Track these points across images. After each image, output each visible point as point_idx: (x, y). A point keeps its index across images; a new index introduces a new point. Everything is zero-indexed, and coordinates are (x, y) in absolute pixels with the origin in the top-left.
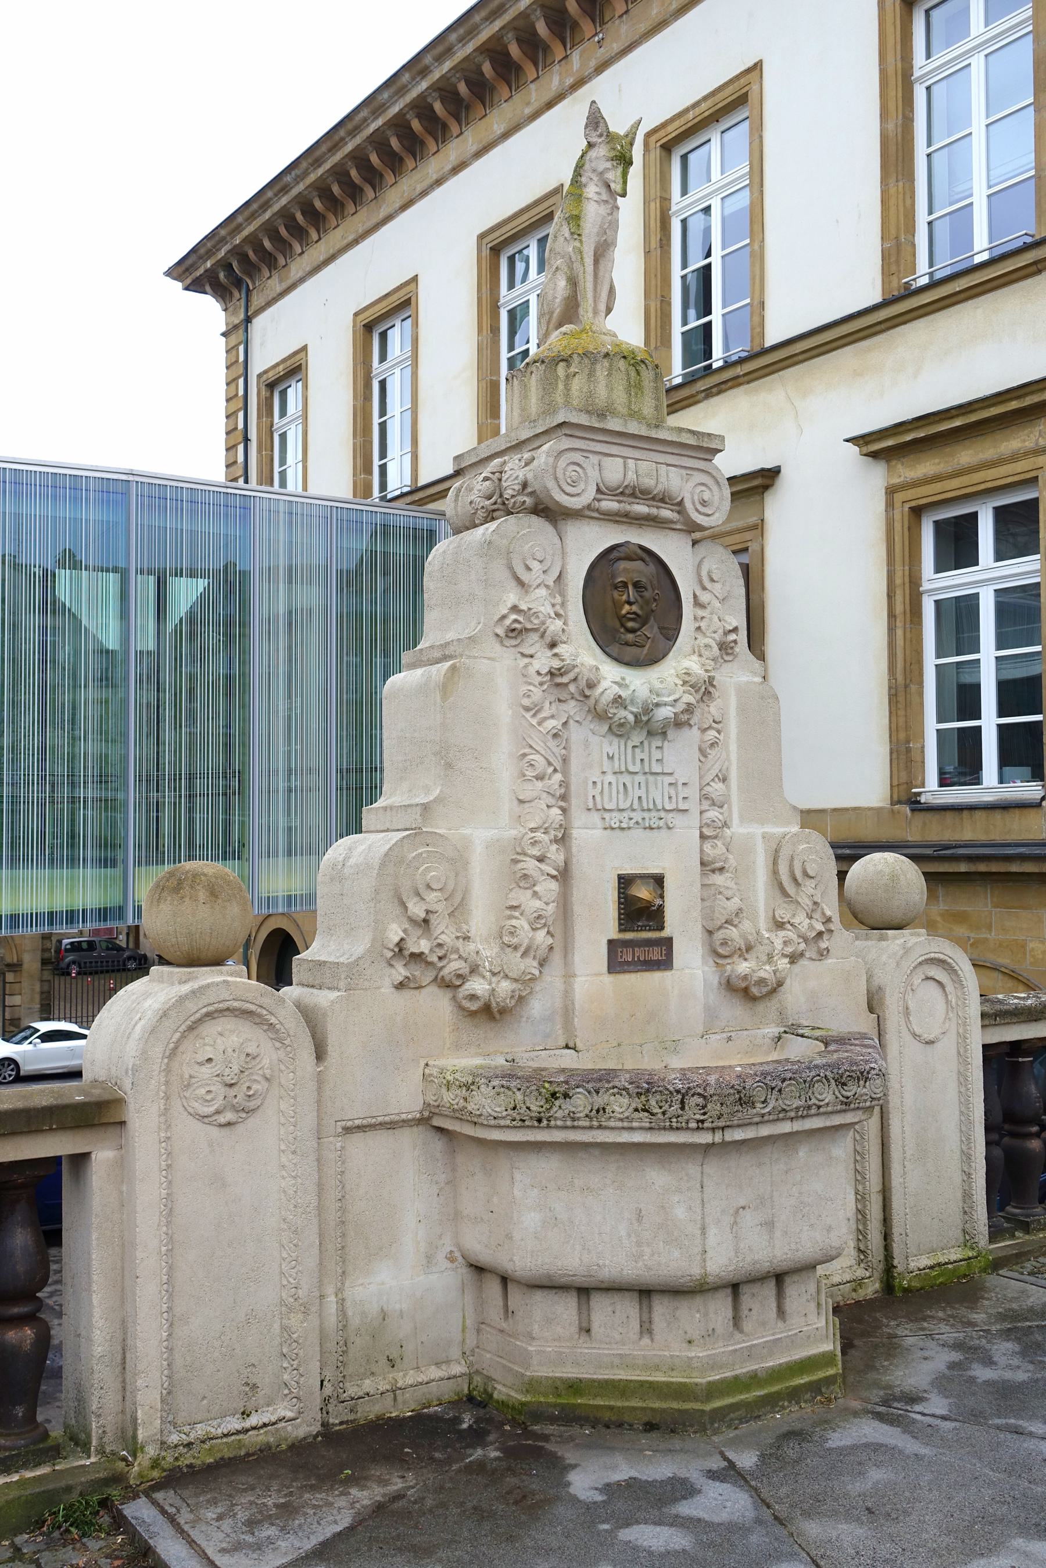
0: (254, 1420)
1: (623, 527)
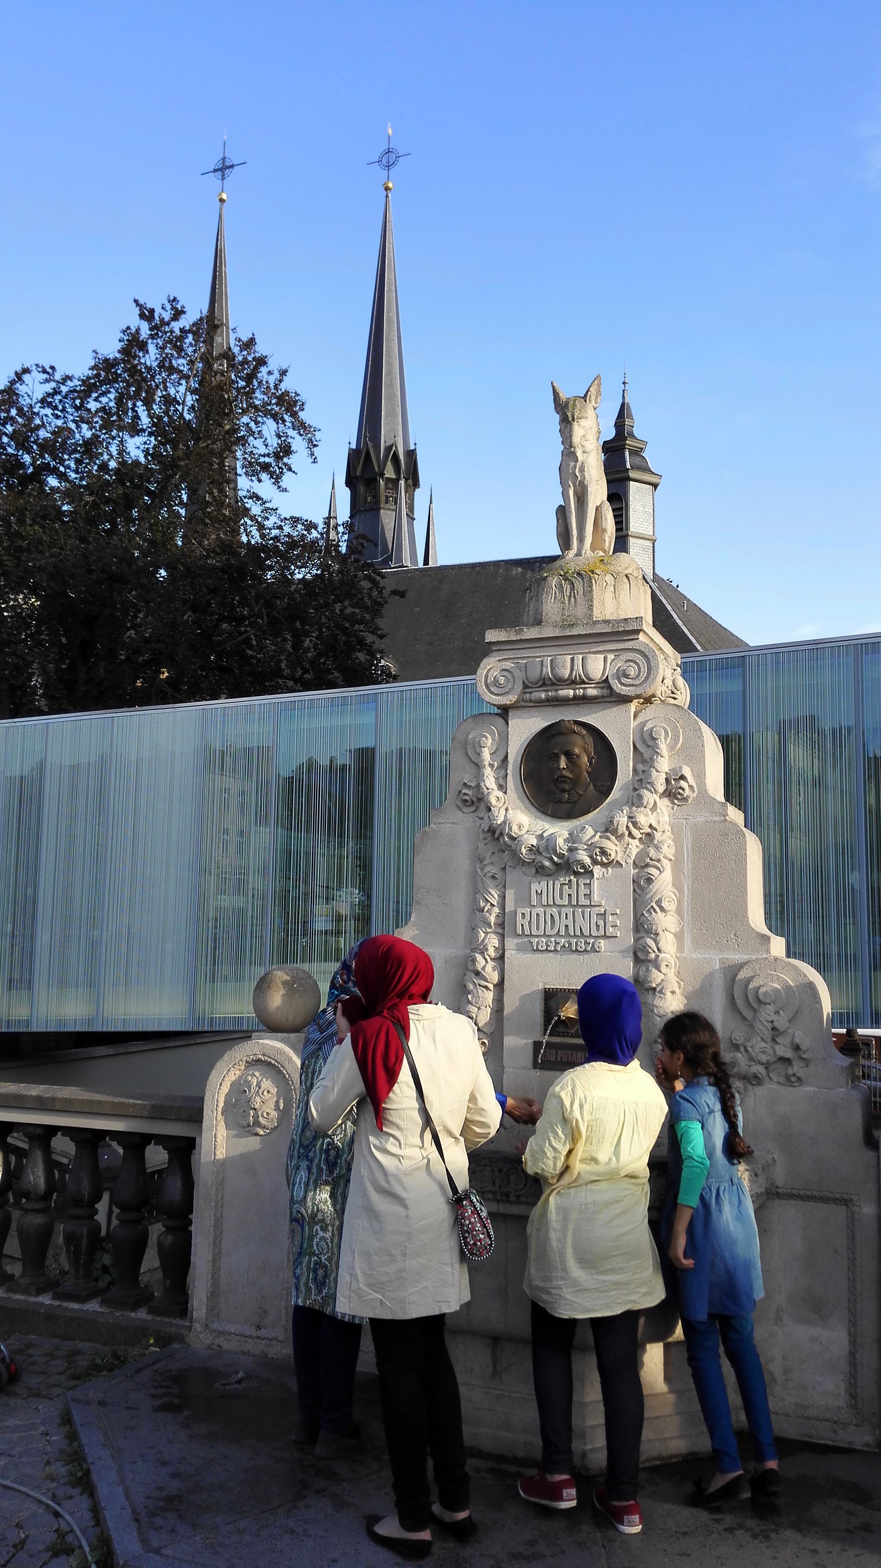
0: (263, 1333)
1: (561, 709)
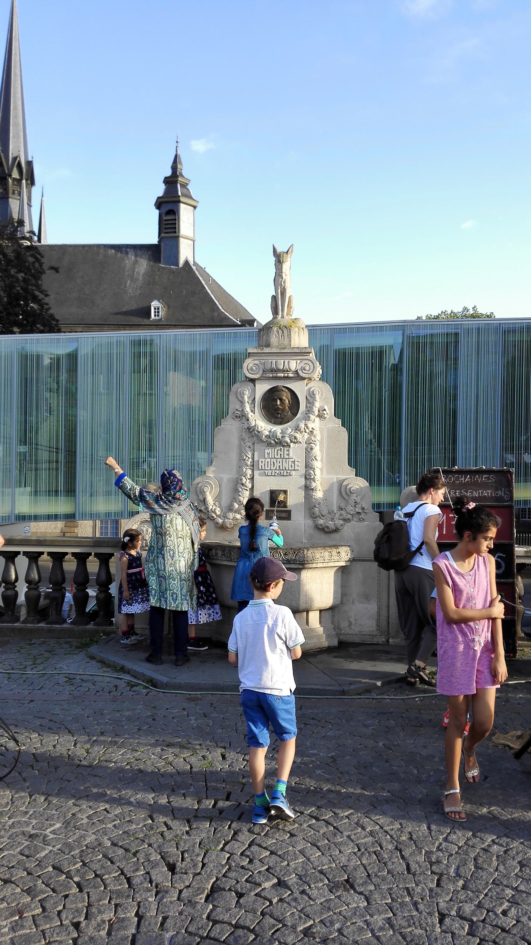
1: (277, 381)
